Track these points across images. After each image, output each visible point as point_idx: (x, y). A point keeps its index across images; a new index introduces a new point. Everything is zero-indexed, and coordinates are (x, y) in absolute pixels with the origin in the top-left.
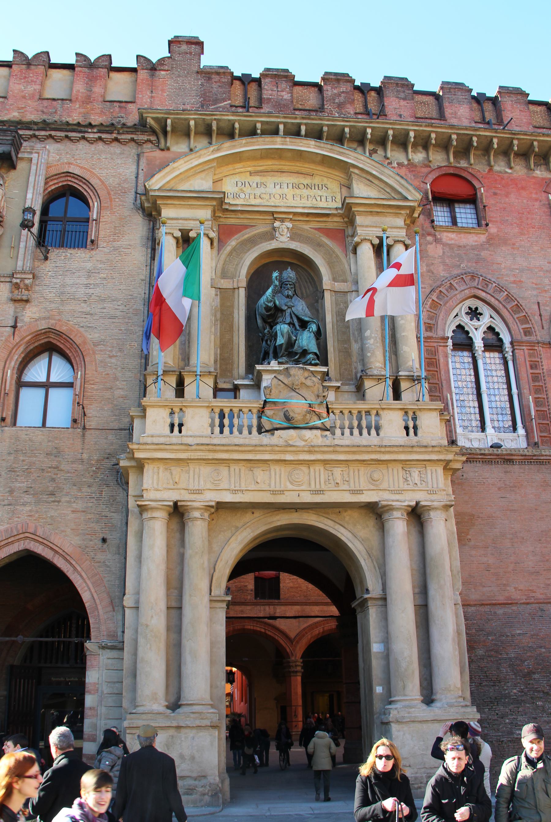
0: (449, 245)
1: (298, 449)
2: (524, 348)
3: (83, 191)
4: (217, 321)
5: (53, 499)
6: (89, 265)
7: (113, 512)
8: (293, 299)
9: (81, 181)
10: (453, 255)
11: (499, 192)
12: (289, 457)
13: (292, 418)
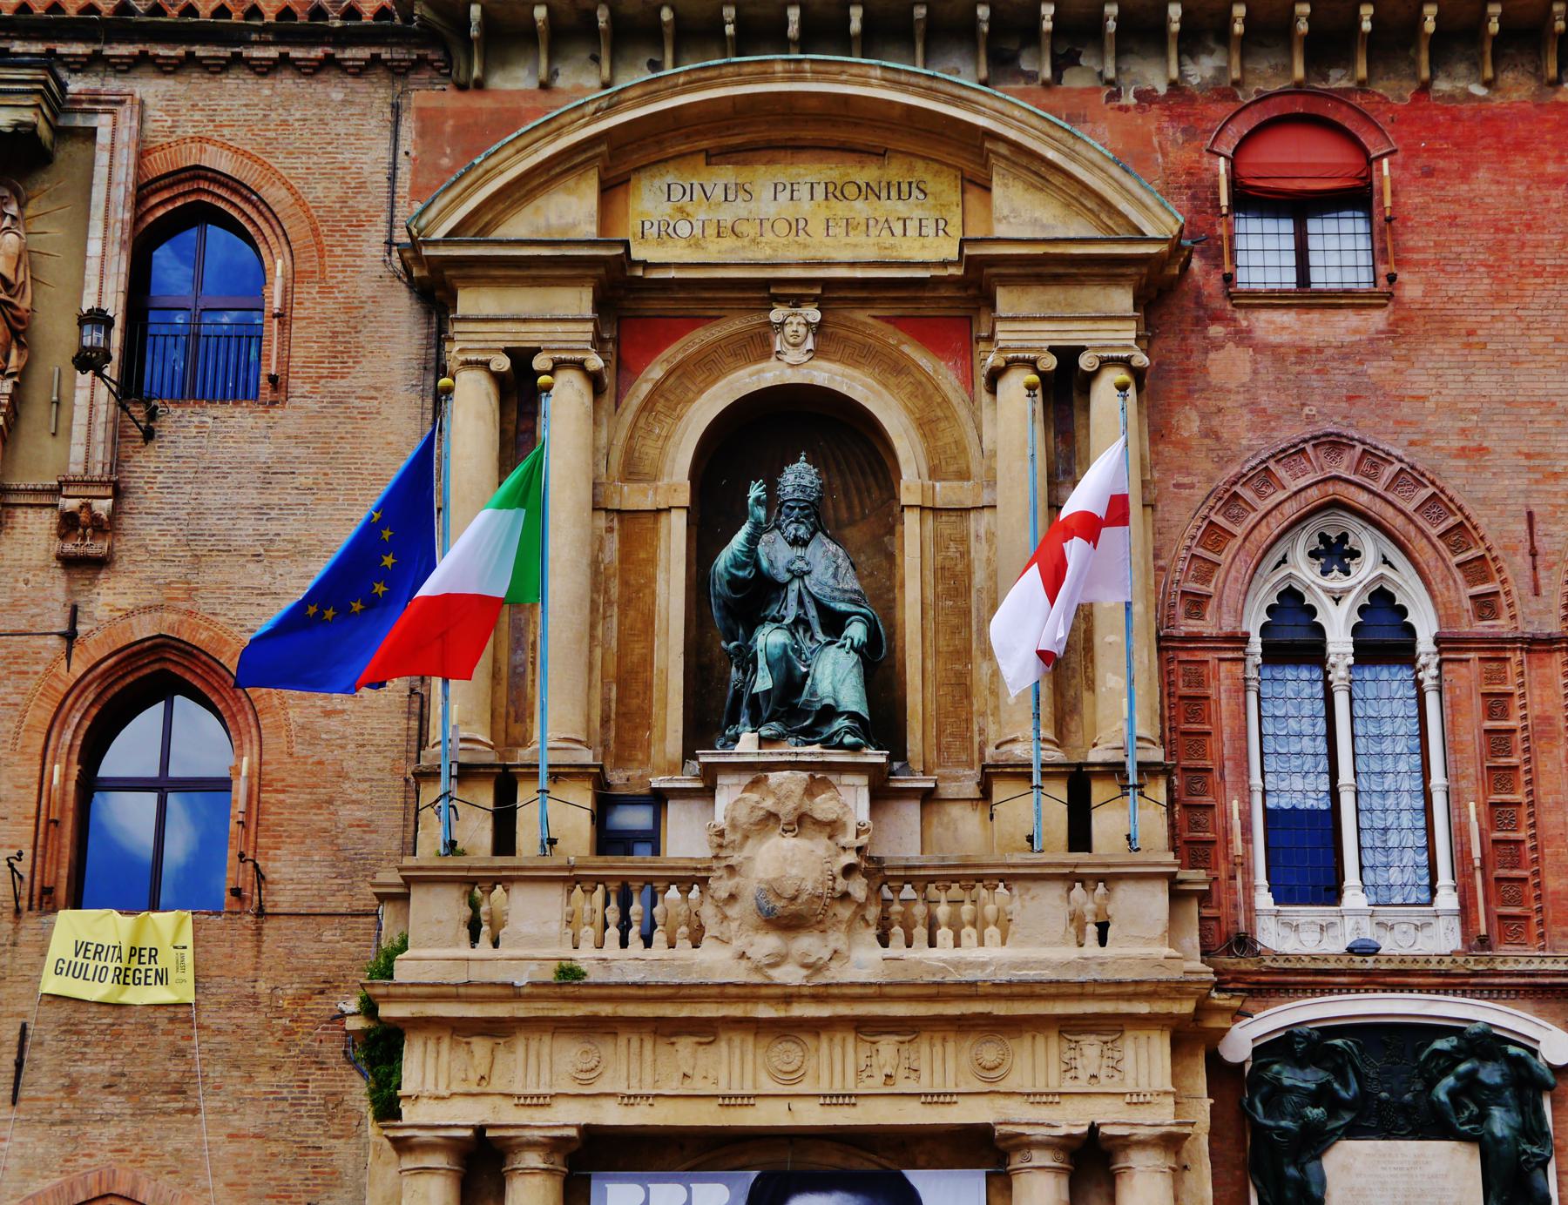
0: (1274, 349)
2: (1471, 655)
3: (242, 220)
5: (181, 1105)
6: (264, 452)
7: (335, 1137)
8: (811, 546)
9: (235, 192)
11: (1441, 164)
12: (764, 1011)
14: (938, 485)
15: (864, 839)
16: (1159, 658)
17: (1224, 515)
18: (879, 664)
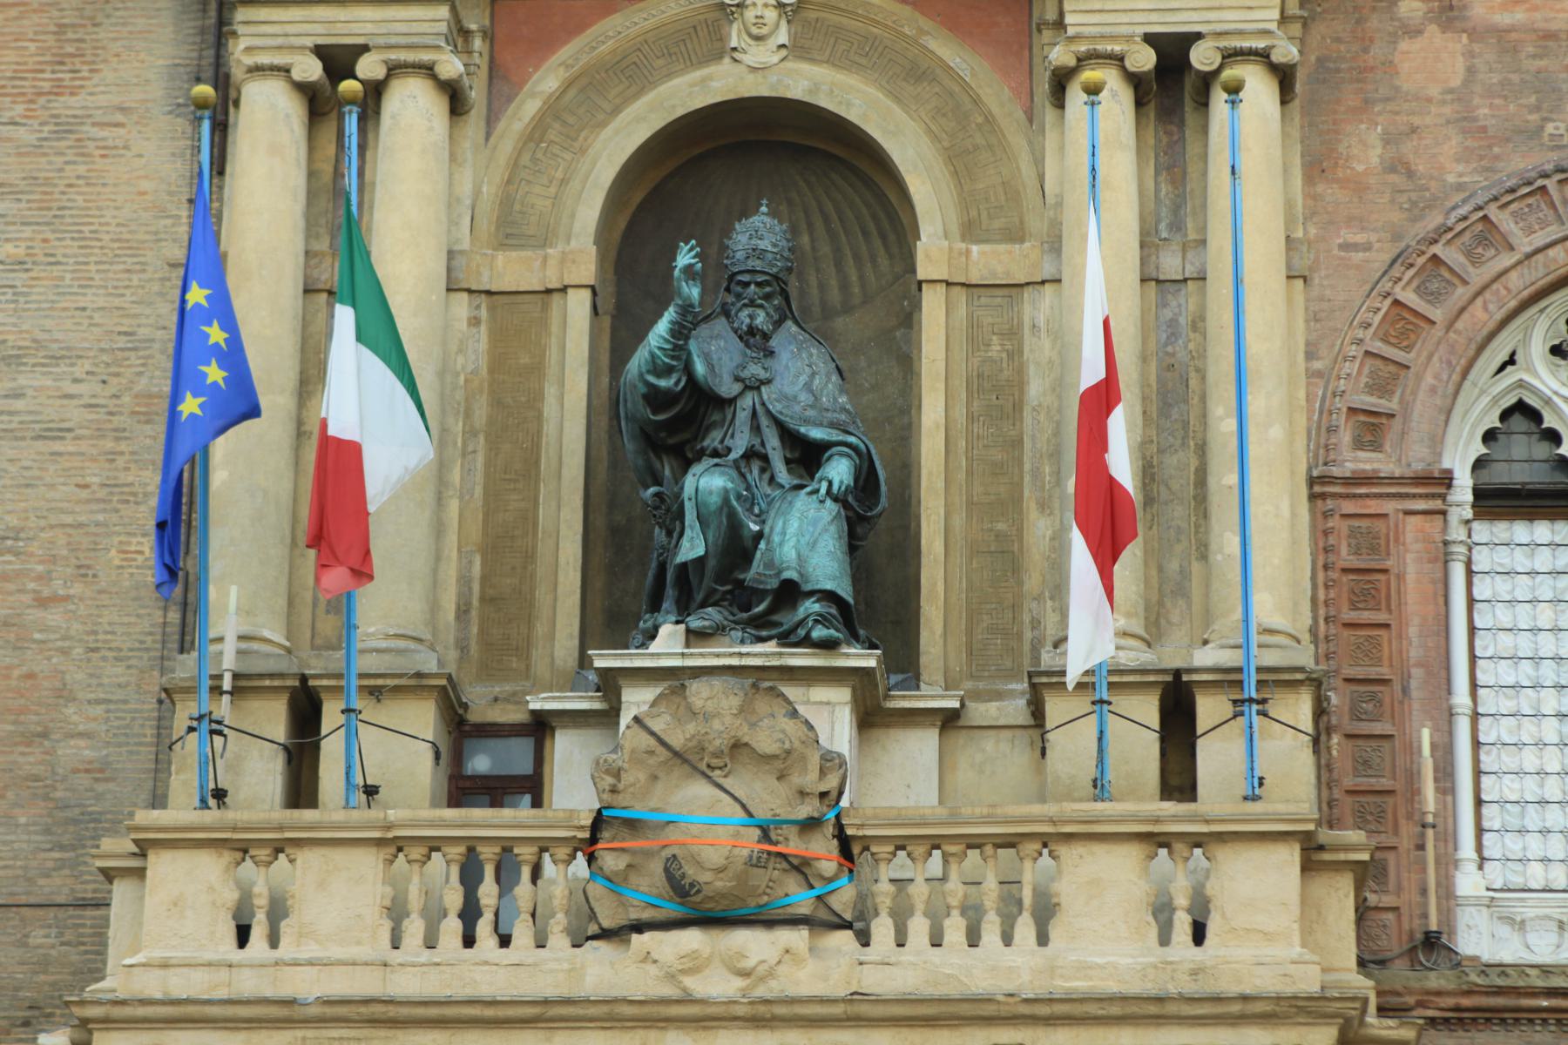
0: (1500, 32)
1: (710, 1010)
4: (475, 434)
10: (1515, 78)
13: (692, 885)
14: (975, 248)
15: (831, 783)
16: (1312, 511)
17: (1417, 290)
18: (876, 517)
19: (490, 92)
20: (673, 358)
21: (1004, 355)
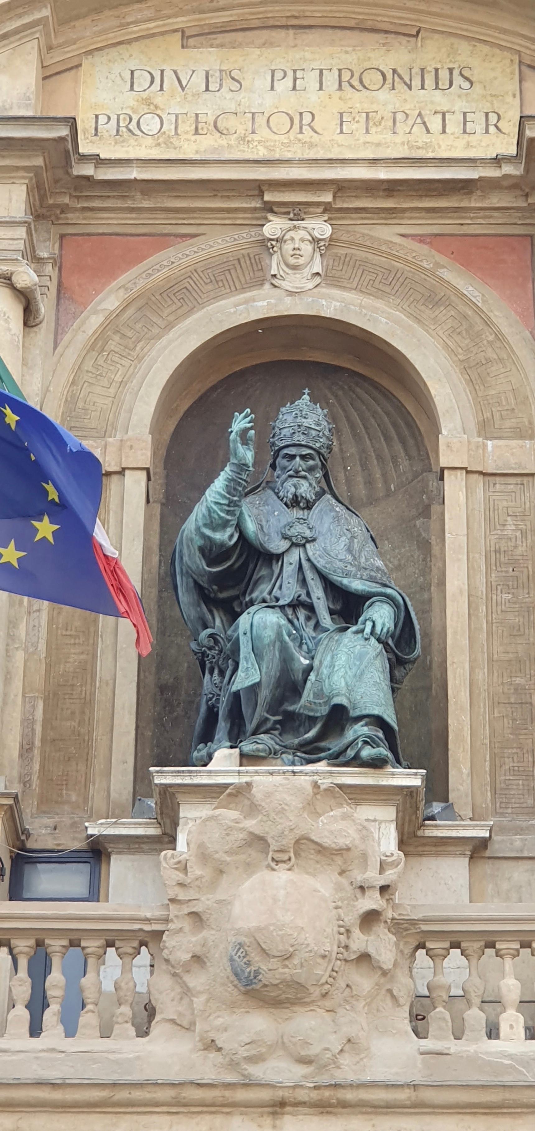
14: (489, 443)
19: (58, 310)
20: (228, 512)
21: (518, 534)
